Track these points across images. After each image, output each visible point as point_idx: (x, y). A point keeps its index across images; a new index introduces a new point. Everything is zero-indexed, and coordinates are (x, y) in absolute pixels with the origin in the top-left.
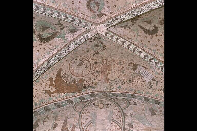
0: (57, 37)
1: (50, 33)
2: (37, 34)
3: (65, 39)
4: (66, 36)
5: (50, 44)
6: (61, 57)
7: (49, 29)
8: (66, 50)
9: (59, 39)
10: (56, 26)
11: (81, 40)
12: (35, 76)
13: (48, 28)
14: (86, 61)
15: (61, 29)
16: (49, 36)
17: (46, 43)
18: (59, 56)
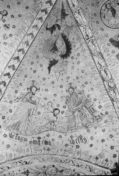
0: (68, 35)
1: (62, 43)
2: (59, 59)
3: (72, 26)
4: (68, 24)
5: (75, 46)
7: (56, 43)
8: (84, 28)
9: (71, 34)
11: (74, 5)
12: (106, 74)
13: (55, 44)
14: (111, 3)
15: (59, 29)
16: (65, 45)
17: (72, 51)
18: (88, 39)
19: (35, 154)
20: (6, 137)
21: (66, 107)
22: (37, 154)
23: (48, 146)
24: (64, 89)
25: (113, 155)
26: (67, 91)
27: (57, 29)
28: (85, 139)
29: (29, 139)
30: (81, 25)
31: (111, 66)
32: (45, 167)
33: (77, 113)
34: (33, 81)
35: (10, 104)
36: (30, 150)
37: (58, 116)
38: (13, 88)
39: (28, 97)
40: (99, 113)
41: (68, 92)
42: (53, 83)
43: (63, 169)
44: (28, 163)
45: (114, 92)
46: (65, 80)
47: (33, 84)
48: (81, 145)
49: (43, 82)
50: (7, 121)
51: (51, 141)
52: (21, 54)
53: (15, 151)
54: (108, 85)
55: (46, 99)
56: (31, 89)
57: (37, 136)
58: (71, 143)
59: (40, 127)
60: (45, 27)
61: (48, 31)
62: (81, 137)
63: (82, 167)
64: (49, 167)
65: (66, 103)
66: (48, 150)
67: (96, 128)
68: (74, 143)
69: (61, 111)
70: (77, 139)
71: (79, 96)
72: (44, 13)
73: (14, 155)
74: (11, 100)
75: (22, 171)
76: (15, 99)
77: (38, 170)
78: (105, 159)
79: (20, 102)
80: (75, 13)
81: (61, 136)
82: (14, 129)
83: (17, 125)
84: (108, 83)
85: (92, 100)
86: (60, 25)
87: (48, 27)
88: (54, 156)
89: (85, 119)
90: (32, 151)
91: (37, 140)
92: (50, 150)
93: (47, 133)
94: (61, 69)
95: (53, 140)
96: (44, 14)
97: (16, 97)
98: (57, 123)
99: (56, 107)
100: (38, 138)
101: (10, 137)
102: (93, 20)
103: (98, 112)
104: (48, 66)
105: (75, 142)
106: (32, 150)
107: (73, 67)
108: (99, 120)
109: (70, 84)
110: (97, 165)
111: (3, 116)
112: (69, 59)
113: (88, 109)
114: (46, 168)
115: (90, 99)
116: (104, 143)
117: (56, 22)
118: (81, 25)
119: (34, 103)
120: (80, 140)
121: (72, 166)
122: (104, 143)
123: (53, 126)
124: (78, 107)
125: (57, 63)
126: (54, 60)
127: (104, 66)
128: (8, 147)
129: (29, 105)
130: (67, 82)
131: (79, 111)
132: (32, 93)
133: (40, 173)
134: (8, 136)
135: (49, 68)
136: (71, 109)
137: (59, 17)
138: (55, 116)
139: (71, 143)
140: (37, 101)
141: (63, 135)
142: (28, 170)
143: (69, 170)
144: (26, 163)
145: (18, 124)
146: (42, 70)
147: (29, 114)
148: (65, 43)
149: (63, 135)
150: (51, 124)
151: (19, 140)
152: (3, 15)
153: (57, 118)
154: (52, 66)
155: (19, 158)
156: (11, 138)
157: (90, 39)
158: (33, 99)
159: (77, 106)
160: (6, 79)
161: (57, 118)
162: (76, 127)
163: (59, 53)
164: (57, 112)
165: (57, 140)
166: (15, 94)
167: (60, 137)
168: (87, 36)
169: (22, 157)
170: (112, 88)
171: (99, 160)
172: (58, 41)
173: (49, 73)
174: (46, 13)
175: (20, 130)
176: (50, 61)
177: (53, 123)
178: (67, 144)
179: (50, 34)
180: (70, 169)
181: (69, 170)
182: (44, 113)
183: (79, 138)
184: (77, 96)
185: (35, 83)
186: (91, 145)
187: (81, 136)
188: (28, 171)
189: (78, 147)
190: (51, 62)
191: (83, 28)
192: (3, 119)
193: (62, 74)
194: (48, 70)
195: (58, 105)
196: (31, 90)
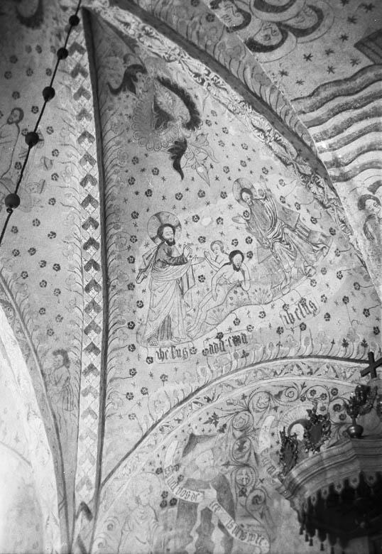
2: (186, 134)
6: (207, 72)
7: (159, 103)
8: (180, 62)
10: (139, 91)
11: (127, 25)
12: (282, 149)
13: (157, 108)
15: (144, 71)
16: (178, 99)
17: (199, 107)
18: (203, 81)
19: (219, 375)
20: (152, 362)
21: (252, 240)
22: (224, 373)
23: (242, 347)
24: (232, 197)
25: (373, 330)
26: (238, 201)
27: (138, 74)
28: (313, 305)
29: (200, 345)
30: (171, 58)
31: (290, 116)
32: (246, 397)
33: (277, 245)
34: (157, 215)
35: (131, 292)
36: (208, 369)
37: (243, 267)
38: (119, 257)
39: (163, 255)
40: (319, 234)
41: (241, 201)
42: (202, 194)
43: (282, 389)
44: (211, 398)
45: (318, 184)
46: (223, 177)
47: (160, 220)
48: (309, 320)
49: (180, 204)
50: (142, 330)
51: (245, 332)
52: (92, 187)
53: (181, 383)
54: (299, 172)
55: (202, 239)
56: (160, 234)
57: (215, 333)
58: (288, 323)
59: (215, 309)
60: (109, 91)
61: (122, 95)
62: (303, 302)
63: (318, 373)
64: (257, 391)
65: (248, 229)
66: (245, 355)
67: (324, 271)
68: (293, 319)
69: (245, 251)
70: (297, 309)
71: (267, 204)
72: (80, 75)
73: (181, 392)
74: (128, 283)
75: (205, 419)
76: (136, 275)
77: (234, 407)
78: (361, 340)
79: (149, 277)
80: (141, 39)
81: (264, 312)
82: (162, 339)
83: (166, 327)
84: (298, 168)
85: (294, 209)
86: (139, 63)
87: (115, 86)
88: (260, 365)
89: (299, 256)
90: (212, 371)
91: (217, 341)
92: (248, 355)
93: (232, 317)
94: (204, 156)
95: (249, 328)
96: (83, 78)
97: (137, 271)
98: (248, 285)
99: (232, 249)
100: (217, 337)
101: (159, 359)
102: (196, 19)
103: (316, 232)
104: (171, 162)
105: (295, 316)
106: (213, 369)
107: (222, 144)
108: (325, 251)
109: (237, 180)
110: (348, 360)
111: (129, 324)
112: (204, 128)
113: (294, 231)
114: (248, 398)
115: (289, 206)
116: (350, 304)
117: (125, 63)
118: (171, 58)
119: (181, 261)
120: (303, 309)
121: (299, 378)
122: (348, 304)
123: (242, 294)
124: (276, 230)
125: (186, 146)
126: (176, 143)
127: (269, 131)
128: (163, 381)
129: (173, 272)
130: (229, 179)
131: (281, 240)
132: (168, 242)
133: (238, 413)
134: (156, 360)
135: (177, 167)
136: (264, 241)
137: (126, 50)
138: (238, 270)
139: (288, 323)
140: (186, 255)
141: (267, 309)
142: (214, 414)
143: (293, 387)
144: (209, 400)
145: (166, 323)
146: (163, 179)
147: (182, 290)
148: (176, 96)
149: (267, 309)
150: (236, 292)
151: (180, 356)
152: (17, 123)
153: (243, 272)
154: (181, 157)
155: (192, 394)
156: (163, 358)
157: (208, 79)
158: (175, 254)
159: (273, 229)
160: (92, 254)
161: (243, 272)
162: (289, 282)
163: (179, 123)
164: (237, 258)
165: (258, 324)
166: (131, 265)
167: (263, 315)
168: (197, 75)
169: (198, 390)
170: (309, 176)
171: (351, 345)
172: (160, 99)
173: (182, 177)
174: (84, 74)
175: (175, 334)
176: (169, 151)
177: (239, 290)
178: (279, 328)
179: (131, 95)
180: (294, 386)
181: (293, 387)
182: (212, 272)
183: (301, 307)
184: (263, 205)
185: (163, 218)
186: (328, 317)
187: (302, 299)
188: (215, 416)
189: (303, 327)
190: (171, 150)
191: (177, 62)
192: (132, 328)
193: (212, 167)
194: (175, 173)
195: (235, 242)
196: (161, 237)
